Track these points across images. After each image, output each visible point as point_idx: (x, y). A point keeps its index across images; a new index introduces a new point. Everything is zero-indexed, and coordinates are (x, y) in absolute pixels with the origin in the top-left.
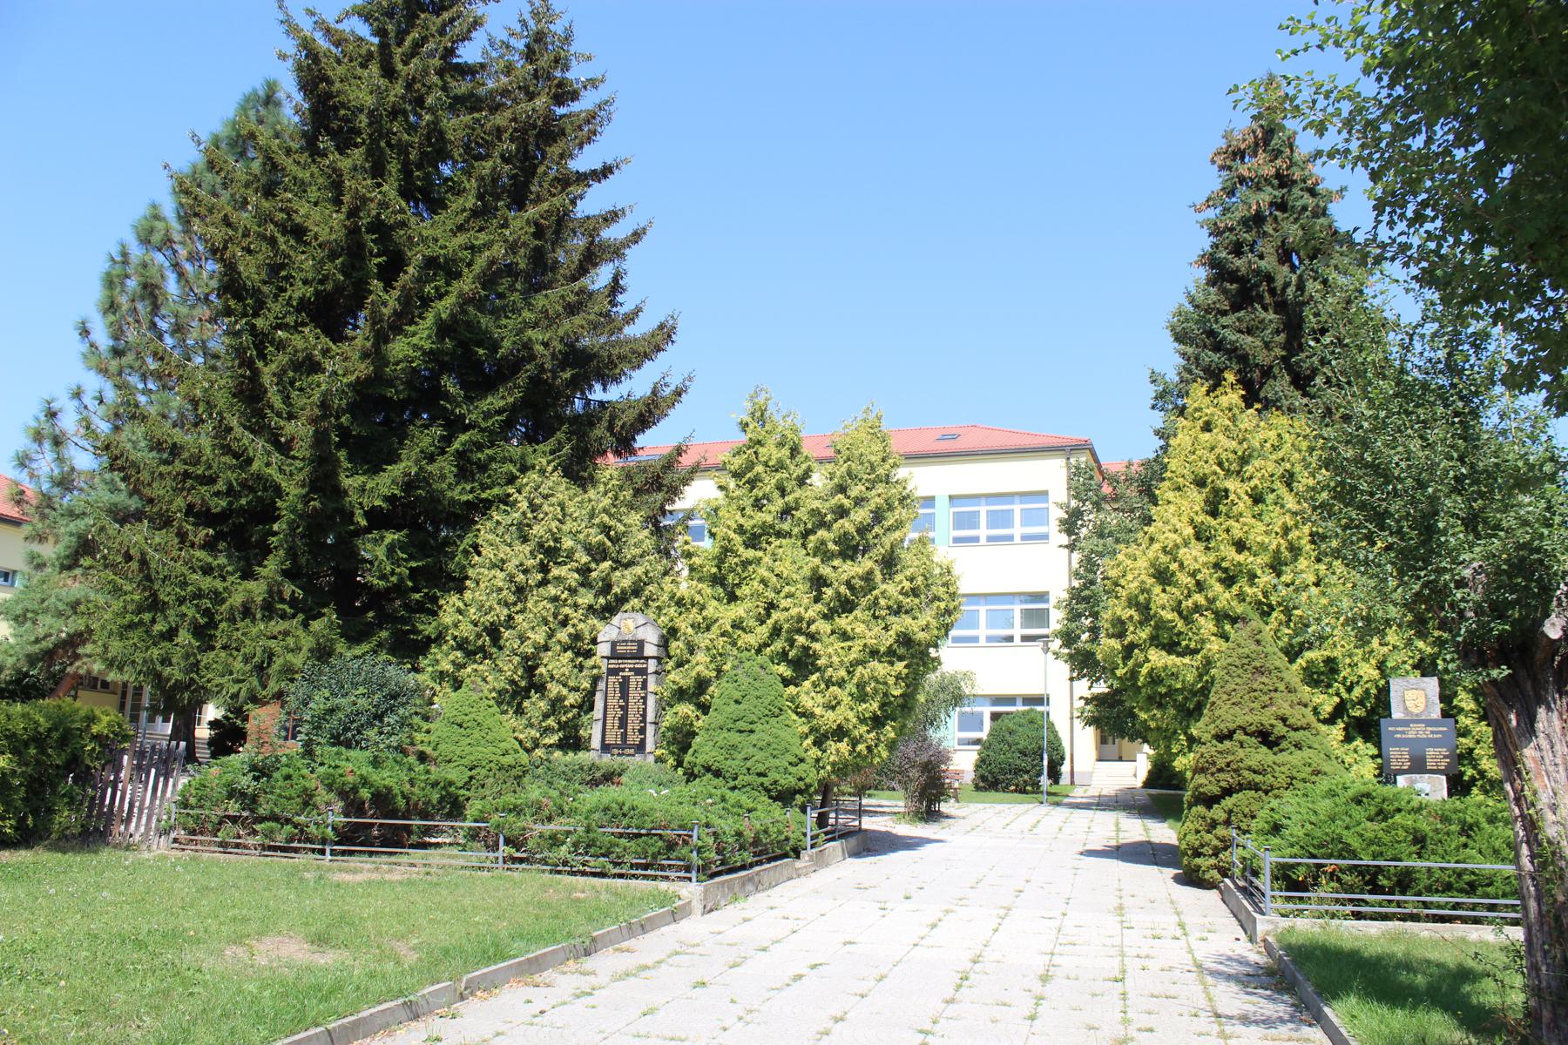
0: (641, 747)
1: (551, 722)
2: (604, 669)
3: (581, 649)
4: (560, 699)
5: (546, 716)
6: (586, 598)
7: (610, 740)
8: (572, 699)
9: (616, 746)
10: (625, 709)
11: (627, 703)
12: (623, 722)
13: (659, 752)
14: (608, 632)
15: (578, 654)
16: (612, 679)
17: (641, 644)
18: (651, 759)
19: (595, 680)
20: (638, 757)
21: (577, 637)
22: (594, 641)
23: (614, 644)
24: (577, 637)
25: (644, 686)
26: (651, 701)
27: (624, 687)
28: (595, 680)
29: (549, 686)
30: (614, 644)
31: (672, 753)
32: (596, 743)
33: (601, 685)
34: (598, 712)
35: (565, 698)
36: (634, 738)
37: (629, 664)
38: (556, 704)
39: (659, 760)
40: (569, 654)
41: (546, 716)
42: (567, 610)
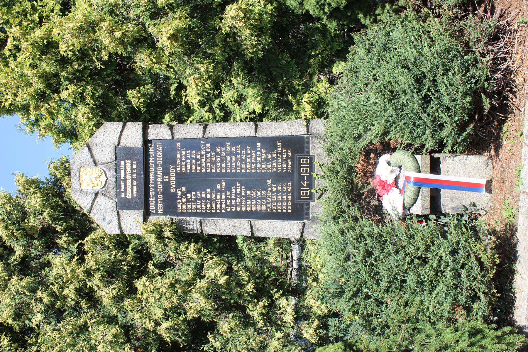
0: (297, 145)
1: (256, 311)
2: (165, 219)
3: (132, 263)
4: (214, 293)
5: (247, 321)
6: (59, 264)
7: (284, 203)
8: (215, 271)
9: (296, 192)
10: (232, 179)
11: (220, 176)
12: (254, 181)
13: (307, 110)
14: (107, 219)
15: (142, 272)
16: (181, 205)
17: (121, 153)
18: (318, 125)
19: (182, 235)
20: (317, 150)
21: (111, 273)
22: (121, 242)
23: (124, 204)
24: (111, 273)
25: (191, 144)
26: (219, 130)
27: (191, 181)
28: (182, 235)
29: (192, 314)
30: (124, 204)
31: (307, 88)
32: (290, 229)
33: (192, 224)
34: (237, 228)
35: (213, 283)
36: (282, 161)
37: (156, 175)
38: (226, 301)
39: (320, 108)
40: (140, 284)
41: (247, 321)
42: (70, 292)
